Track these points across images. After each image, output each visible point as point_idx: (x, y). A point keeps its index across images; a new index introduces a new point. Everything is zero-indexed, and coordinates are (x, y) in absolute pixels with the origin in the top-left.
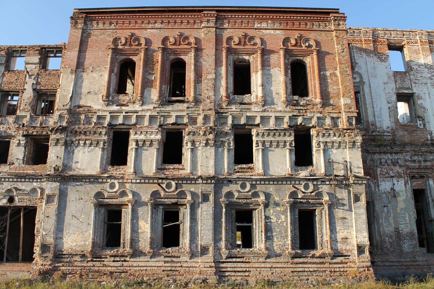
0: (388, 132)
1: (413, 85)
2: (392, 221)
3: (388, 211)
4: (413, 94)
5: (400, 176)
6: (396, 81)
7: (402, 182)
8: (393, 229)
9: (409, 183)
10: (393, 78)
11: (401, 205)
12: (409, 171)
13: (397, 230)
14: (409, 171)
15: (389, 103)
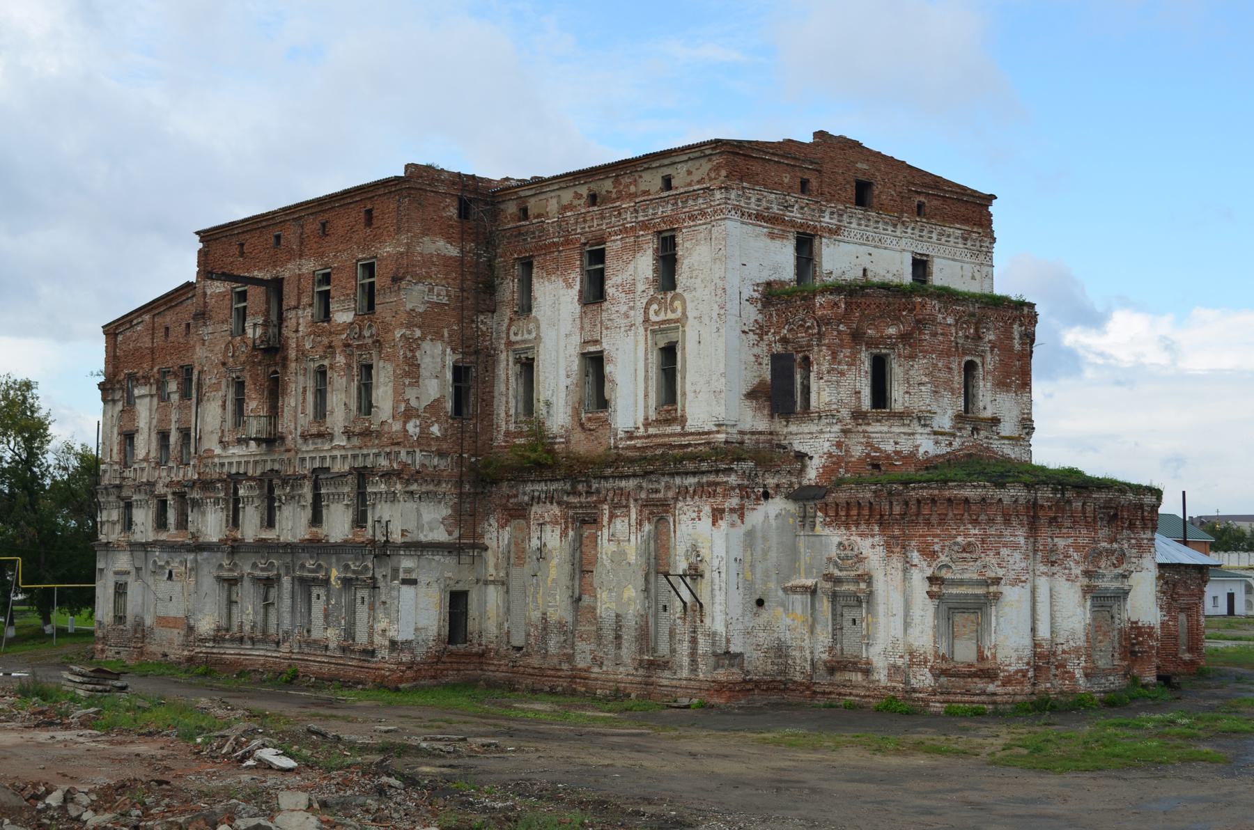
0: (561, 437)
1: (605, 332)
2: (540, 601)
3: (538, 584)
4: (602, 352)
5: (557, 523)
6: (582, 328)
7: (558, 532)
8: (538, 614)
9: (571, 533)
10: (578, 321)
11: (553, 573)
12: (571, 513)
13: (544, 617)
14: (571, 513)
15: (568, 376)
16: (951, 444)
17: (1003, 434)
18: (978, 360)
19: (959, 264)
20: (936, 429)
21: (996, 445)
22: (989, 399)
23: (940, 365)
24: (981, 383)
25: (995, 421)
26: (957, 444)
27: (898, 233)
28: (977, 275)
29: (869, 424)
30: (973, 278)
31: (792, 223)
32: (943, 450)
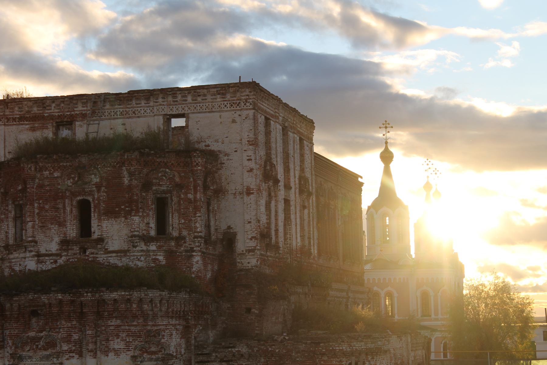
16: (56, 262)
17: (111, 249)
18: (90, 199)
19: (217, 114)
20: (43, 251)
21: (101, 258)
22: (96, 225)
23: (47, 207)
24: (92, 215)
25: (101, 240)
26: (61, 261)
27: (152, 104)
28: (238, 119)
29: (12, 253)
30: (234, 121)
31: (51, 117)
32: (48, 265)
